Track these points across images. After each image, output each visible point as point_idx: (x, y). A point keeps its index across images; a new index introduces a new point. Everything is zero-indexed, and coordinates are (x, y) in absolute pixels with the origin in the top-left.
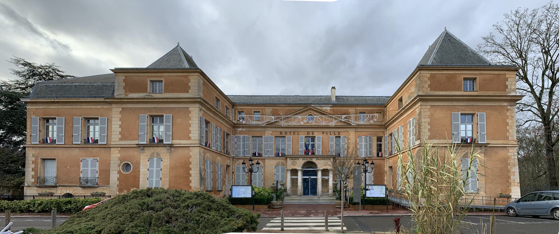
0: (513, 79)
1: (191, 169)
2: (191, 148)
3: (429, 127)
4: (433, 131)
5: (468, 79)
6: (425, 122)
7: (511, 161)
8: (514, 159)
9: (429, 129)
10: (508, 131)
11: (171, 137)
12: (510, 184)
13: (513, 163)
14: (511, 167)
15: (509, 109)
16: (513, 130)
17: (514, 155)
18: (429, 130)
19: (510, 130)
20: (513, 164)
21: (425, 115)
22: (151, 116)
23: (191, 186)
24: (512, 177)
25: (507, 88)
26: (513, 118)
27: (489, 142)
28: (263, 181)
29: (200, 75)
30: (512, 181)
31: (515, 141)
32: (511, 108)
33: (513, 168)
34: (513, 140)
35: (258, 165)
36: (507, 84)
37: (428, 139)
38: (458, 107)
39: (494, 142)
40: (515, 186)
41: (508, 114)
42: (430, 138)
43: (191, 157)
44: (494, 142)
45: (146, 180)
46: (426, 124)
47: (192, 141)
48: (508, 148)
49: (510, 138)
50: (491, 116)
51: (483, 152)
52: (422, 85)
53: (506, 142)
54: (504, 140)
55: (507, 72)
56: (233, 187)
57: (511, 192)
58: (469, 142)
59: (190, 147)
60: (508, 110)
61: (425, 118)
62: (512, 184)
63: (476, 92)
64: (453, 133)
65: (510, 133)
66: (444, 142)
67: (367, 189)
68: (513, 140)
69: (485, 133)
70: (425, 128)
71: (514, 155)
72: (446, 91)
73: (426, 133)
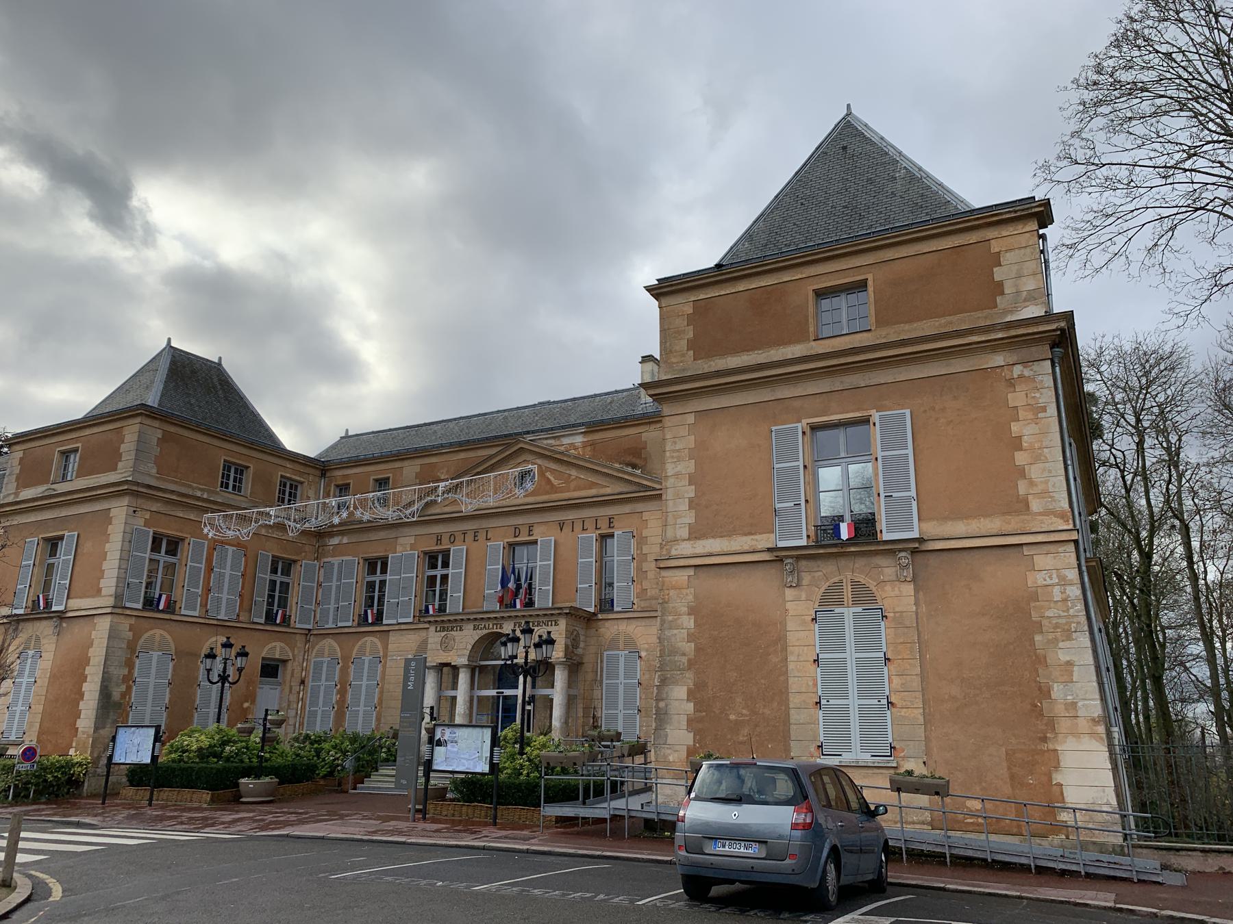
0: (1023, 251)
2: (96, 620)
3: (690, 492)
5: (842, 291)
6: (677, 475)
7: (1049, 613)
8: (1065, 600)
9: (691, 501)
10: (1022, 473)
11: (67, 591)
12: (1051, 724)
13: (1063, 621)
14: (1049, 642)
15: (1020, 377)
16: (1047, 465)
17: (1064, 582)
18: (692, 504)
19: (1033, 467)
20: (1057, 626)
21: (678, 451)
22: (46, 540)
24: (1057, 691)
25: (1002, 293)
26: (1040, 415)
27: (932, 528)
28: (376, 707)
29: (148, 421)
30: (1059, 709)
31: (1062, 516)
32: (1027, 373)
33: (1061, 645)
34: (1048, 513)
35: (209, 661)
36: (997, 278)
37: (689, 539)
38: (797, 403)
39: (959, 528)
40: (1076, 735)
41: (1016, 398)
42: (696, 534)
43: (91, 645)
44: (959, 528)
45: (6, 709)
46: (683, 483)
48: (1026, 551)
49: (1035, 505)
50: (937, 419)
51: (908, 573)
52: (668, 344)
53: (1014, 523)
54: (1004, 514)
55: (990, 233)
57: (1057, 767)
58: (844, 535)
60: (1011, 383)
61: (679, 459)
62: (1063, 725)
63: (865, 334)
64: (778, 506)
65: (1032, 483)
66: (746, 548)
68: (1048, 513)
69: (913, 493)
71: (1064, 582)
72: (748, 351)
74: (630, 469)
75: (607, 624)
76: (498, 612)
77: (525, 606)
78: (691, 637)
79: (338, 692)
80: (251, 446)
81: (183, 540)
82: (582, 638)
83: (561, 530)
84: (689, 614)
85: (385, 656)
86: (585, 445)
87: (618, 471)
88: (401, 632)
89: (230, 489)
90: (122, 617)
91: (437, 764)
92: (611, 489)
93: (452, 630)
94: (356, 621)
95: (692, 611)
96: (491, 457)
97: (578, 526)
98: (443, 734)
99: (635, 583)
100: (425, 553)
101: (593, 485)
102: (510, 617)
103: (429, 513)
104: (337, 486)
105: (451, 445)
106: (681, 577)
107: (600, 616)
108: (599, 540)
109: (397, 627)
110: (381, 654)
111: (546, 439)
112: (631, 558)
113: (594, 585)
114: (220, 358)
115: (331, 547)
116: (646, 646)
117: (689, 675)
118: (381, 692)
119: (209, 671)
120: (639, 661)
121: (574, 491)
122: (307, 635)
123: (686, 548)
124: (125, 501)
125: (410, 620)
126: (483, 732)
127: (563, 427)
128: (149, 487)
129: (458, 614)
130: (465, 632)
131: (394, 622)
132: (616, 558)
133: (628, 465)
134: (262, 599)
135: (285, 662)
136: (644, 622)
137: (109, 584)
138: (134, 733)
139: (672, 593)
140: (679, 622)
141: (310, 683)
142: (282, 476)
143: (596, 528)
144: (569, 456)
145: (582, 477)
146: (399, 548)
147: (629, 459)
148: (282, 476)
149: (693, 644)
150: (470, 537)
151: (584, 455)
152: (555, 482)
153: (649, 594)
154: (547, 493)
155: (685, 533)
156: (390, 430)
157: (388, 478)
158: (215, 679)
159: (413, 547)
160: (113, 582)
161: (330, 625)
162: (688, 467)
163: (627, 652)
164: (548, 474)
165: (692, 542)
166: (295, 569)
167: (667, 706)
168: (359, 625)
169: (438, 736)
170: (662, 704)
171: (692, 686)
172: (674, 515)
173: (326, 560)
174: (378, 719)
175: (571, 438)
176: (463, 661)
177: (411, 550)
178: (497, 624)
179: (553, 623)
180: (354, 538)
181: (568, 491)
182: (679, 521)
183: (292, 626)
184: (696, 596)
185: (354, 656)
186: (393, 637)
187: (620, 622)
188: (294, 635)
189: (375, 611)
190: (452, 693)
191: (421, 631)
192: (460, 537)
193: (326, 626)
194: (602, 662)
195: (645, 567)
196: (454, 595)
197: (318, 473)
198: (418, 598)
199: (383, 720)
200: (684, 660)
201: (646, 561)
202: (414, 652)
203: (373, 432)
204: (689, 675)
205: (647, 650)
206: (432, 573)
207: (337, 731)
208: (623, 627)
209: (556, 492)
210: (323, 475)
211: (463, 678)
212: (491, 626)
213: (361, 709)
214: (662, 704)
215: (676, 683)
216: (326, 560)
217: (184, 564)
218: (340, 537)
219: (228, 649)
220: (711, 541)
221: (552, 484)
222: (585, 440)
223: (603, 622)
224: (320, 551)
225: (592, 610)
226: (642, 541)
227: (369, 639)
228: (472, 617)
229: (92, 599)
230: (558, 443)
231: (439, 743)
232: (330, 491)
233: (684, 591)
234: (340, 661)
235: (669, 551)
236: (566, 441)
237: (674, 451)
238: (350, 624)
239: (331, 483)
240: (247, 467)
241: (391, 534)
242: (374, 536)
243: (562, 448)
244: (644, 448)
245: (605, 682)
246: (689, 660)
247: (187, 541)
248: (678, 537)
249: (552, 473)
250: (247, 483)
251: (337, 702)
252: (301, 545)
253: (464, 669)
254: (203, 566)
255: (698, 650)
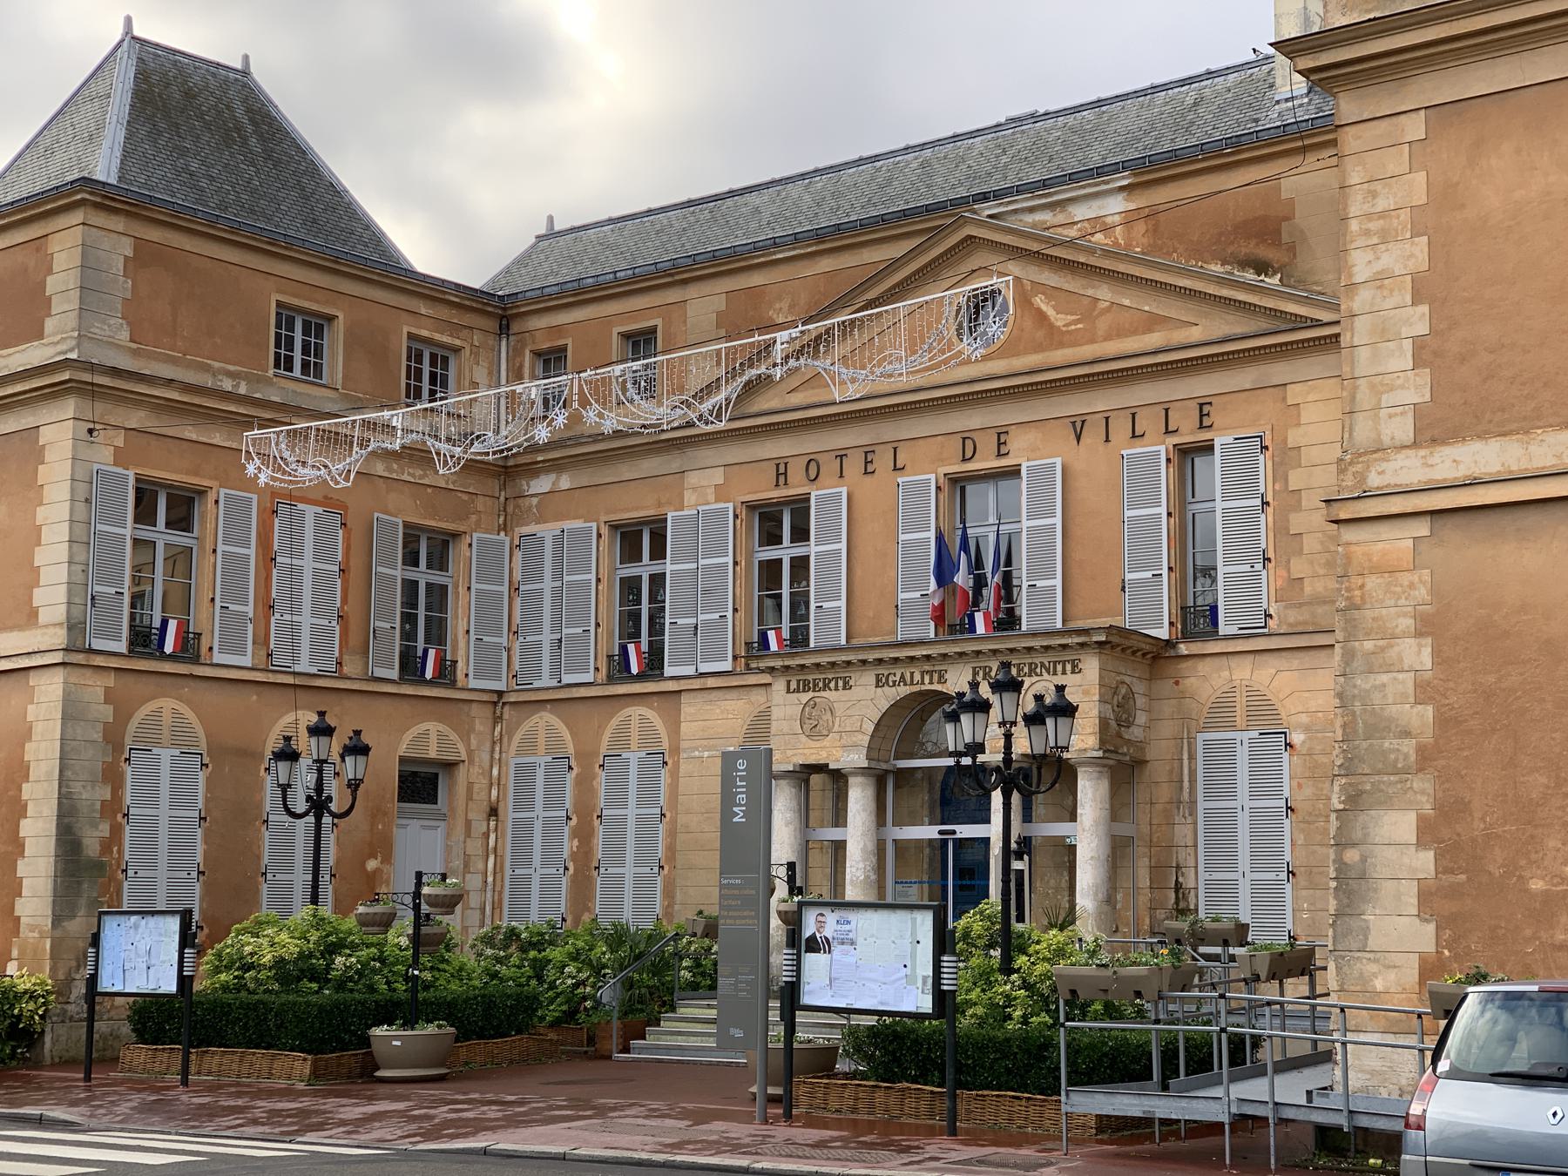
1: (23, 813)
2: (34, 679)
3: (1418, 321)
4: (1463, 360)
6: (1379, 279)
9: (1419, 344)
18: (1423, 354)
21: (1383, 215)
23: (19, 918)
28: (661, 867)
29: (100, 219)
35: (283, 767)
37: (1415, 445)
43: (28, 735)
47: (39, 631)
56: (107, 920)
59: (32, 673)
61: (1386, 237)
67: (813, 938)
70: (1384, 334)
73: (1392, 389)
74: (1250, 276)
75: (1204, 667)
76: (931, 643)
77: (997, 629)
78: (1424, 690)
79: (575, 833)
80: (335, 265)
81: (202, 493)
82: (1141, 701)
83: (1078, 439)
84: (1419, 634)
85: (676, 750)
86: (1129, 219)
87: (1220, 281)
88: (705, 694)
89: (297, 371)
90: (88, 672)
91: (810, 992)
92: (1203, 328)
93: (826, 687)
94: (604, 671)
95: (1426, 626)
96: (895, 264)
97: (1121, 428)
98: (821, 925)
99: (1271, 566)
100: (751, 507)
101: (1154, 322)
102: (961, 654)
103: (755, 409)
104: (537, 354)
105: (797, 239)
106: (1397, 541)
107: (1183, 649)
108: (1176, 460)
109: (697, 684)
110: (666, 745)
111: (1031, 210)
112: (1258, 502)
113: (1165, 572)
114: (246, 58)
115: (535, 501)
116: (1304, 719)
117: (1423, 785)
118: (672, 834)
119: (285, 788)
120: (1286, 755)
121: (1108, 338)
122: (495, 704)
123: (1407, 469)
124: (69, 407)
125: (727, 666)
126: (914, 921)
127: (1072, 178)
128: (115, 372)
129: (837, 649)
130: (856, 693)
131: (690, 671)
132: (1219, 505)
133: (1244, 264)
134: (388, 624)
135: (450, 766)
136: (1296, 661)
137: (52, 599)
138: (136, 927)
139: (1372, 582)
140: (1392, 653)
141: (509, 814)
142: (411, 336)
143: (1167, 432)
144: (1091, 251)
145: (1127, 302)
146: (690, 498)
147: (1248, 248)
148: (411, 336)
149: (1430, 709)
150: (854, 465)
151: (1128, 246)
152: (1059, 320)
153: (1308, 590)
154: (1039, 348)
155: (1403, 429)
156: (650, 212)
157: (653, 330)
158: (301, 806)
159: (721, 493)
160: (61, 594)
161: (546, 681)
162: (1410, 255)
163: (1255, 734)
164: (1039, 301)
165: (1422, 452)
166: (460, 554)
167: (1364, 859)
168: (611, 680)
169: (809, 929)
170: (1351, 856)
171: (1428, 809)
172: (1372, 387)
173: (526, 530)
174: (669, 893)
175: (1096, 204)
176: (858, 759)
177: (716, 501)
178: (931, 673)
179: (1069, 667)
180: (586, 477)
181: (1092, 341)
182: (1386, 400)
183: (459, 684)
184: (1434, 591)
185: (603, 751)
186: (690, 707)
187: (1234, 661)
188: (465, 707)
189: (644, 647)
190: (834, 834)
191: (755, 691)
192: (830, 466)
193: (536, 684)
194: (1192, 757)
195: (1297, 522)
196: (825, 605)
197: (492, 325)
198: (741, 614)
199: (679, 897)
200: (1408, 747)
201: (1298, 507)
202: (741, 739)
203: (611, 221)
204: (1423, 785)
205: (1307, 729)
206: (770, 553)
207: (577, 922)
208: (1243, 672)
209: (1061, 345)
210: (504, 329)
211: (859, 798)
212: (917, 677)
213: (629, 871)
214: (1351, 856)
215: (1387, 803)
216: (526, 530)
217: (209, 548)
218: (553, 476)
219: (324, 740)
220: (1476, 446)
221: (1051, 326)
222: (1132, 206)
223: (1190, 663)
224: (510, 509)
225: (1163, 633)
226: (1286, 458)
227: (636, 712)
228: (871, 656)
229: (21, 634)
230: (1061, 218)
231: (813, 945)
232: (521, 366)
233: (1405, 578)
234: (573, 764)
235: (1361, 478)
236: (1081, 212)
237: (1369, 216)
238: (589, 678)
239: (523, 348)
240: (331, 319)
241: (671, 463)
242: (626, 471)
243: (1072, 233)
244: (1287, 219)
245: (1201, 805)
246: (1421, 749)
247: (211, 497)
248: (1386, 441)
249: (1049, 298)
250: (333, 356)
251: (574, 856)
252: (465, 497)
253: (859, 779)
254: (252, 552)
255: (1444, 722)
